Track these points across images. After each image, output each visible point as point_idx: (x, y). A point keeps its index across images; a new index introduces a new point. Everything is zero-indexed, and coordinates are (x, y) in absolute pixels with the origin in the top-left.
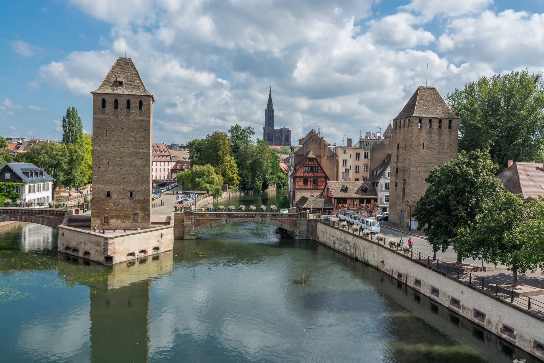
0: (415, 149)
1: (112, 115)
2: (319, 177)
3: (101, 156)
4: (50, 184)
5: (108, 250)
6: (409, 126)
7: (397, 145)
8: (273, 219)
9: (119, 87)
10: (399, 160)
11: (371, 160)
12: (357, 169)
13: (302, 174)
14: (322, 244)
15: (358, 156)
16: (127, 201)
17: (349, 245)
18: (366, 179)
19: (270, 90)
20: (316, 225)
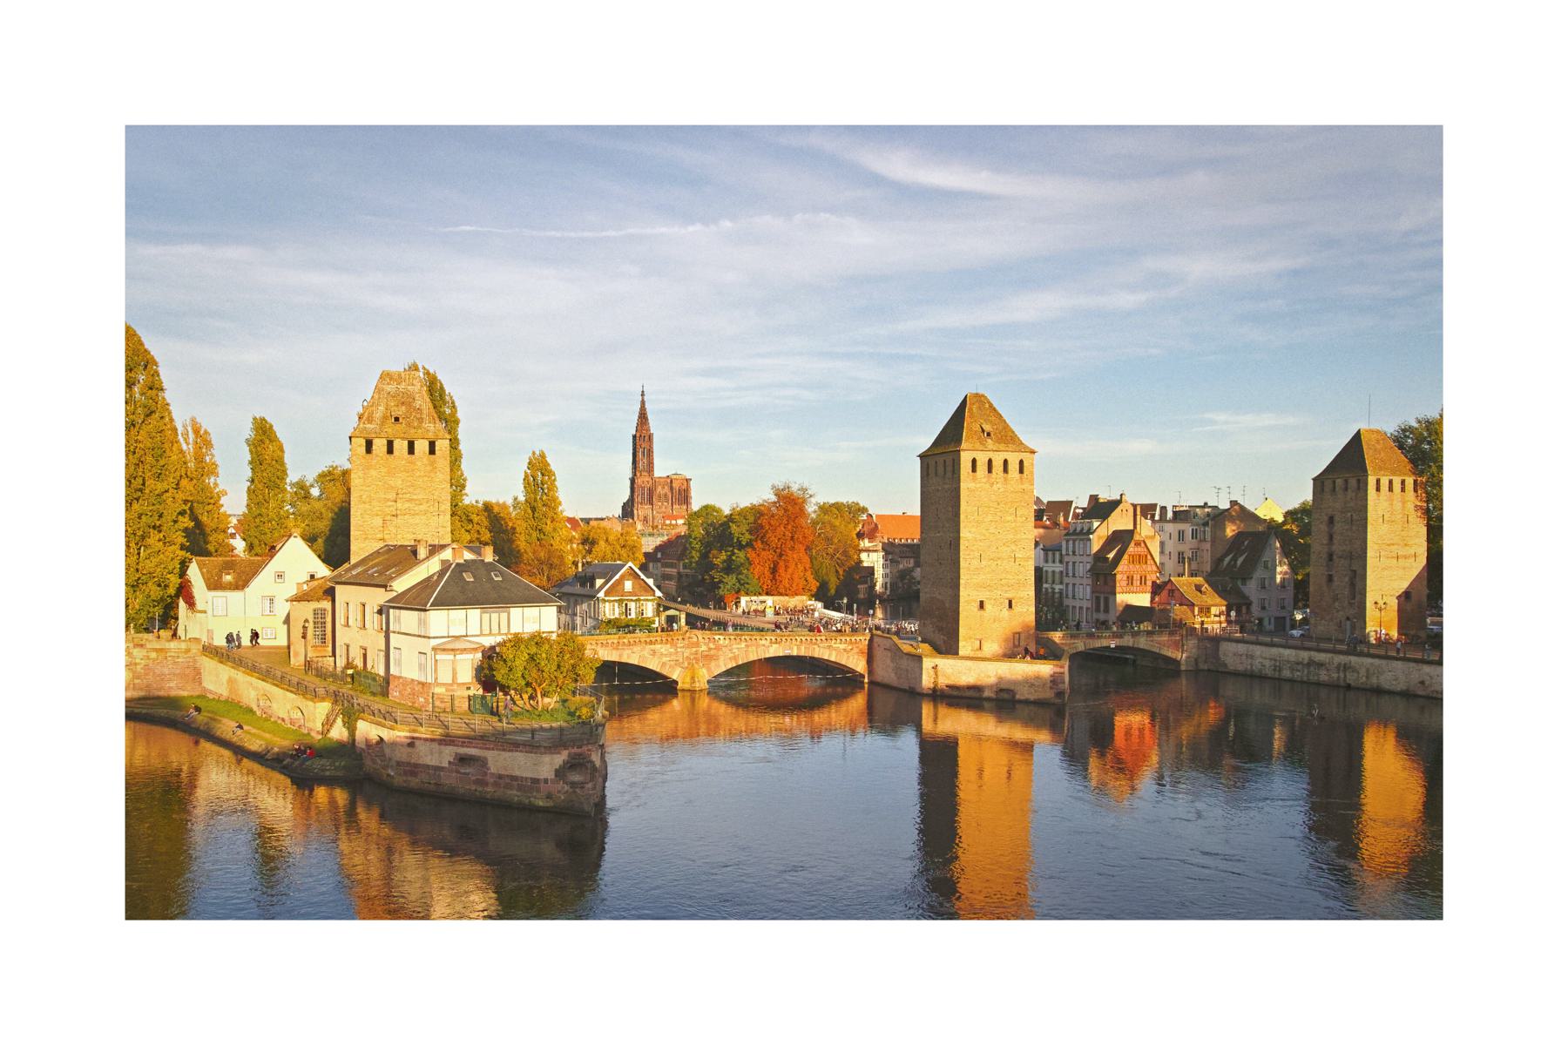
0: (1372, 524)
6: (1359, 488)
7: (1326, 518)
10: (1335, 541)
11: (1213, 541)
14: (1236, 674)
15: (1181, 535)
16: (1005, 612)
17: (1324, 668)
19: (643, 392)
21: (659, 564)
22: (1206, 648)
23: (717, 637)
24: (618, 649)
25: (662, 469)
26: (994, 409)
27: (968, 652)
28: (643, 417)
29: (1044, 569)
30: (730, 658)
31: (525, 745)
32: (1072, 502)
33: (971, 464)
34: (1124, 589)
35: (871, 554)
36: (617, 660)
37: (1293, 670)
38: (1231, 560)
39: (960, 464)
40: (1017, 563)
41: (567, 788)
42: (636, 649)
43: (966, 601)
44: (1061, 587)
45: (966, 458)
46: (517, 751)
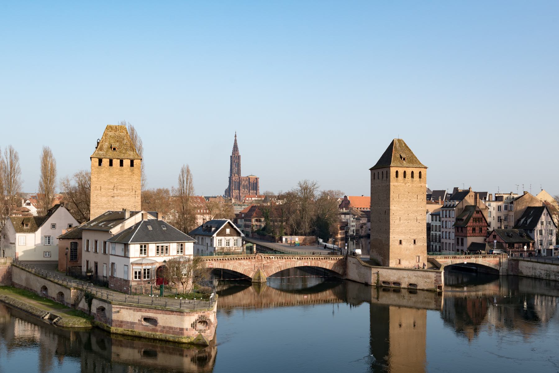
1: (403, 183)
8: (483, 259)
13: (472, 224)
14: (527, 277)
16: (412, 245)
18: (507, 227)
19: (236, 135)
21: (243, 220)
22: (512, 264)
23: (271, 257)
24: (223, 263)
26: (407, 147)
28: (235, 148)
29: (431, 224)
30: (278, 267)
31: (176, 312)
32: (445, 191)
33: (395, 174)
34: (471, 234)
35: (346, 215)
36: (222, 268)
37: (556, 276)
38: (524, 221)
39: (390, 174)
40: (418, 222)
41: (197, 333)
42: (232, 262)
43: (393, 240)
44: (440, 233)
45: (393, 170)
46: (172, 314)
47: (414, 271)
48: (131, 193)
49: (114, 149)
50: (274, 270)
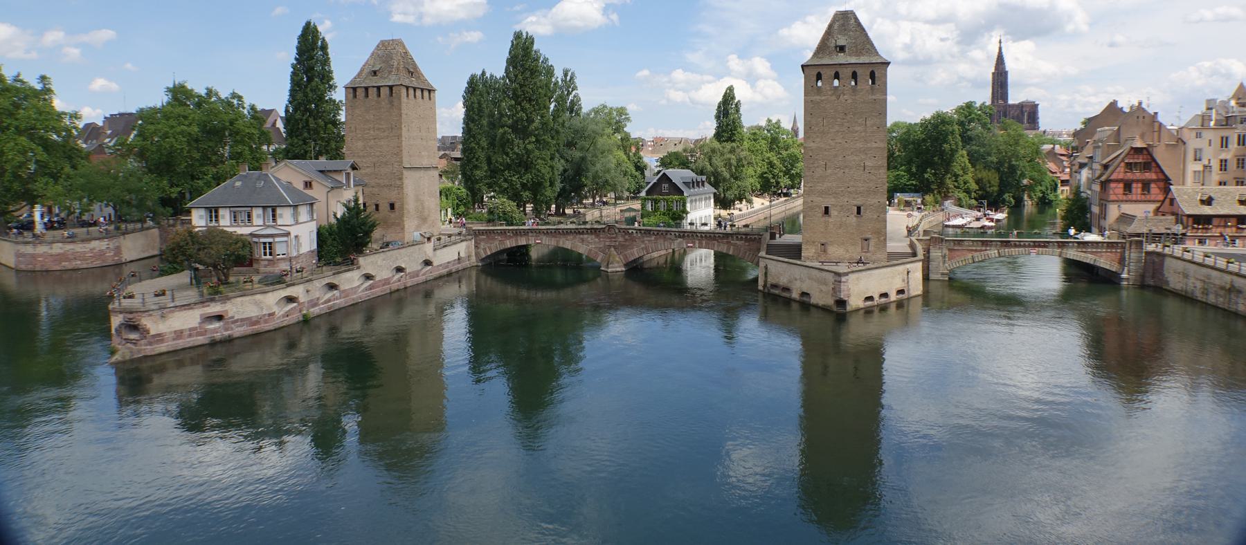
1: (831, 95)
2: (1154, 181)
3: (816, 155)
4: (712, 196)
5: (840, 292)
9: (839, 54)
12: (1224, 165)
13: (1121, 176)
15: (1224, 142)
16: (853, 219)
18: (1242, 182)
20: (1162, 264)
22: (1154, 263)
23: (630, 231)
25: (1014, 98)
27: (809, 254)
28: (1000, 60)
34: (1121, 197)
41: (124, 342)
42: (570, 237)
43: (809, 207)
47: (807, 269)
48: (391, 135)
49: (375, 73)
50: (636, 253)
